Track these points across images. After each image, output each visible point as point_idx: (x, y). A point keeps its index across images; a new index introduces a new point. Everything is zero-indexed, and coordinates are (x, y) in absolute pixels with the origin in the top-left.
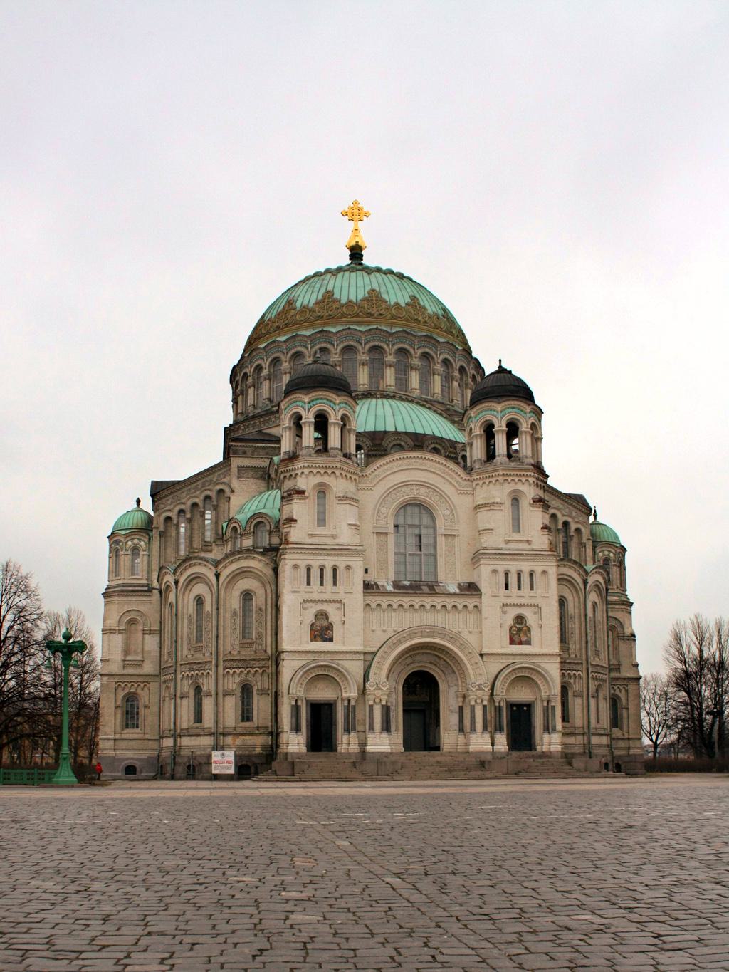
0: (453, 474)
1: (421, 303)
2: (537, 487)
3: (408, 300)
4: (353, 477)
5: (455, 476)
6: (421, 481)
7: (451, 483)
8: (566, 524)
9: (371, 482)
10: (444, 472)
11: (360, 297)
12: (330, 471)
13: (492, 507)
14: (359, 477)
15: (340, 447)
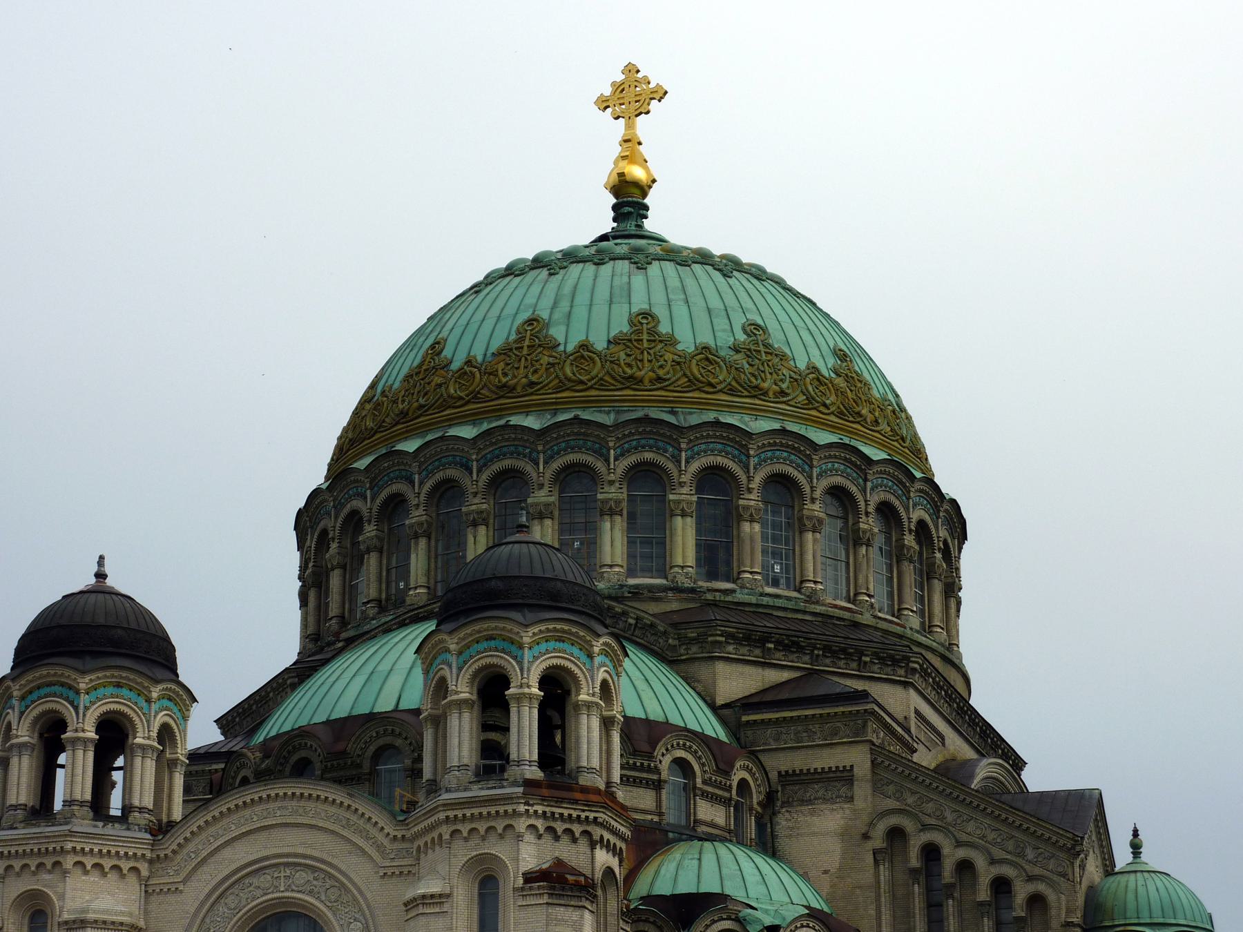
0: (368, 827)
1: (664, 328)
2: (557, 838)
3: (621, 326)
4: (125, 865)
5: (374, 832)
6: (296, 855)
7: (363, 850)
8: (1001, 886)
9: (177, 872)
10: (348, 825)
11: (496, 344)
12: (49, 862)
13: (421, 910)
14: (151, 862)
15: (88, 797)
